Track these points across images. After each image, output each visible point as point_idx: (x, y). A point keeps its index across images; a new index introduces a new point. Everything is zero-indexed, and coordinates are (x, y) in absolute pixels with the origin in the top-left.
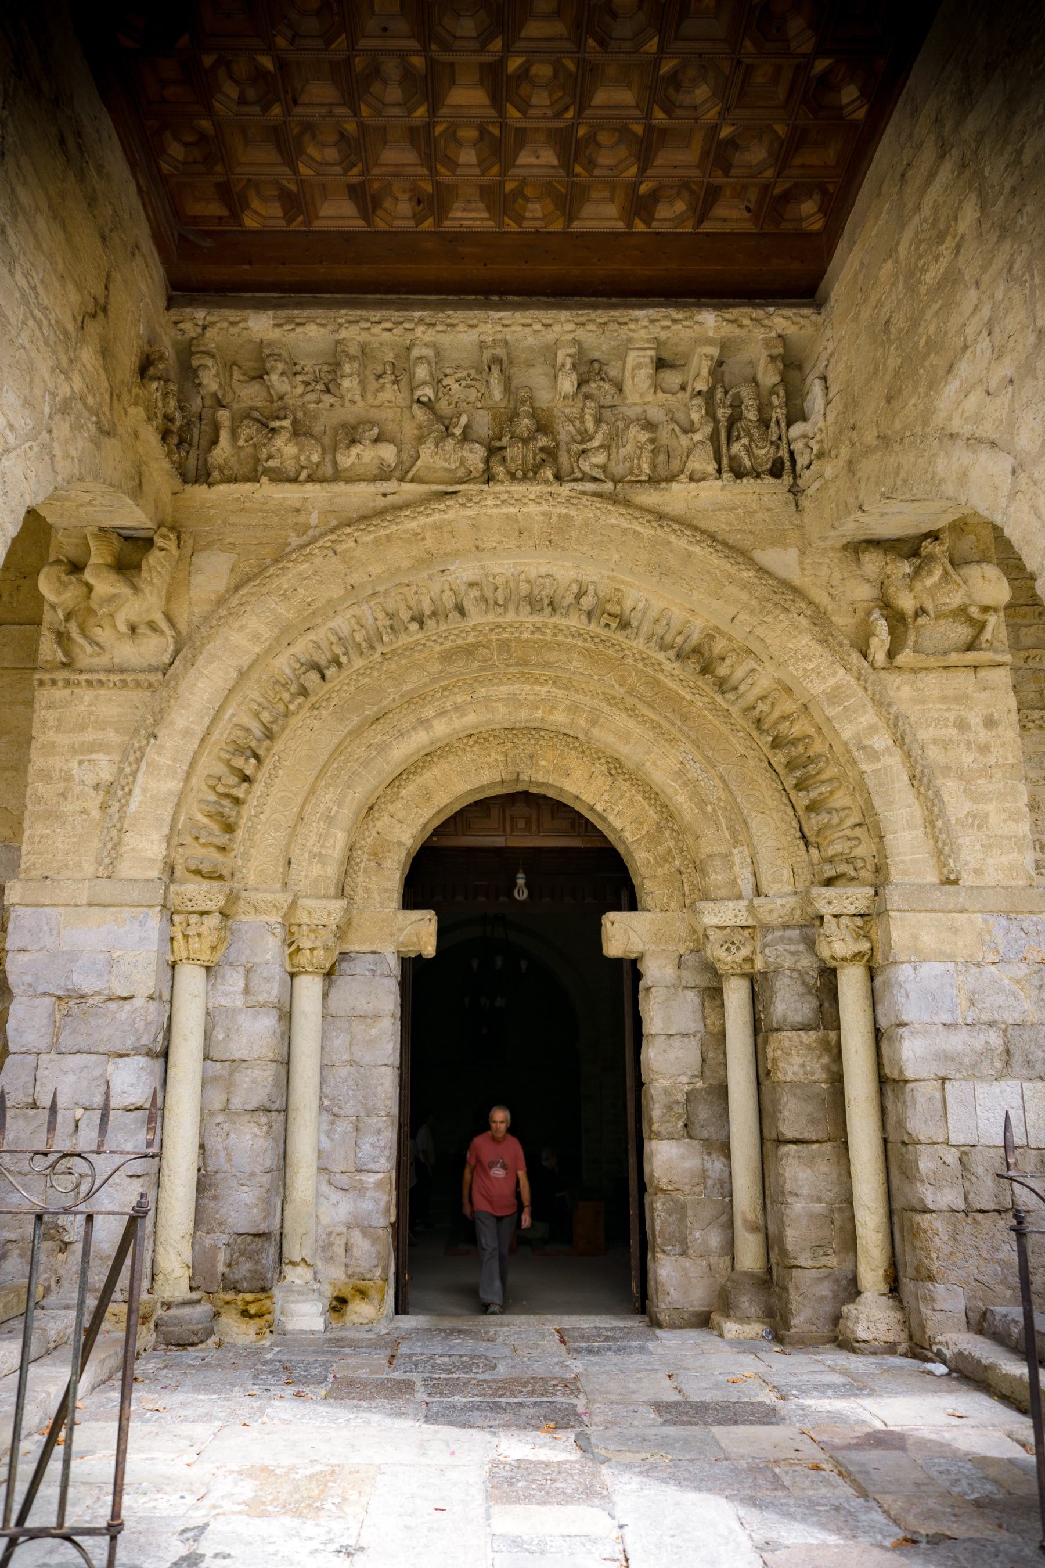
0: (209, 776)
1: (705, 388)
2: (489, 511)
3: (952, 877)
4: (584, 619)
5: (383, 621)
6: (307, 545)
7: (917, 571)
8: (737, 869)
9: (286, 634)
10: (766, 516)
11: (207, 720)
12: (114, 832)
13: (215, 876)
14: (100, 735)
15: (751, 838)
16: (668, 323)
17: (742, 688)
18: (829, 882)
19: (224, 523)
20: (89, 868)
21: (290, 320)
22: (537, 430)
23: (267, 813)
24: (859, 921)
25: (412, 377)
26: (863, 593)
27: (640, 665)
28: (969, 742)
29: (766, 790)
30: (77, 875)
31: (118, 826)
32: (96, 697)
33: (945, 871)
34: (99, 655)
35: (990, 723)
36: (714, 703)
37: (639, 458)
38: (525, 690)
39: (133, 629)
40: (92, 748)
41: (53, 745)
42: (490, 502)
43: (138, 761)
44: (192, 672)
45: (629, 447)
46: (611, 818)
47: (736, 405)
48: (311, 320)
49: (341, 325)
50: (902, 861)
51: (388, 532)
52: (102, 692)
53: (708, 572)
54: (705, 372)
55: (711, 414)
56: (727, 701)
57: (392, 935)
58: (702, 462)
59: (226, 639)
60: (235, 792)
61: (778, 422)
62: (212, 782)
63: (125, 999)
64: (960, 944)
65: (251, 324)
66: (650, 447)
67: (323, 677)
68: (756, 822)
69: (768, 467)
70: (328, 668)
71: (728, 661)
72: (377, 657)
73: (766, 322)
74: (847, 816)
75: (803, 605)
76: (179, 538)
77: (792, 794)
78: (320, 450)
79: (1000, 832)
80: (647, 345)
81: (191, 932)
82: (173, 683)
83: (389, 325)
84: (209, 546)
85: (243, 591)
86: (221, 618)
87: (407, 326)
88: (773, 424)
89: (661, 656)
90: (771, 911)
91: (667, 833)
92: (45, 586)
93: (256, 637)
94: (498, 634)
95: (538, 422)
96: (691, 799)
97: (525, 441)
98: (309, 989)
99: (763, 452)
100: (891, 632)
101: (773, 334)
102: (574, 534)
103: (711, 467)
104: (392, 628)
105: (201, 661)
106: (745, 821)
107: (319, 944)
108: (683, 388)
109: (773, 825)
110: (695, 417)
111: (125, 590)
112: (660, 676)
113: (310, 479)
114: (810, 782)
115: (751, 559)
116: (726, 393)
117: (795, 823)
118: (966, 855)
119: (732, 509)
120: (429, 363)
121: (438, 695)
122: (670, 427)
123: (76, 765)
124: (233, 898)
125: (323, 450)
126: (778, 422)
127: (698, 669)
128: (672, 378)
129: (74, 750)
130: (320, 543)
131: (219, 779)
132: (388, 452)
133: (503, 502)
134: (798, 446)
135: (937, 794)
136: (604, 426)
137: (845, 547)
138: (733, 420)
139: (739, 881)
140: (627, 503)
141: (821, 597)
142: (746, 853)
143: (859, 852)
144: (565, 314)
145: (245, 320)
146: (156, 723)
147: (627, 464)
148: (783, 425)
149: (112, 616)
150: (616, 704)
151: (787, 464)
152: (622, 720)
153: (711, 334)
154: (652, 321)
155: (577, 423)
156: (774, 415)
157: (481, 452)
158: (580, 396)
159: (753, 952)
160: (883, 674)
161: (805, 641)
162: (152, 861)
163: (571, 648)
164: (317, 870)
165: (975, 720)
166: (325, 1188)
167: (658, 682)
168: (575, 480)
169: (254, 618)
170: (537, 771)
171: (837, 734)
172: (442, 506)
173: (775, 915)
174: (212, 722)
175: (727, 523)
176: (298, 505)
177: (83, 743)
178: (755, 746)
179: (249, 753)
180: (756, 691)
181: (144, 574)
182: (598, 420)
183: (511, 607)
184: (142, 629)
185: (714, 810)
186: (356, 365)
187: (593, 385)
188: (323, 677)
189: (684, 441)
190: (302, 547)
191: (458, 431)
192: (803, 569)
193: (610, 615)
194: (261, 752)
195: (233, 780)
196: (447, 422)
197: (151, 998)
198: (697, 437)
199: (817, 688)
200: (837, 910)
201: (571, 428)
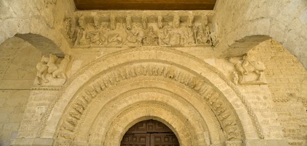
7: (243, 63)
9: (93, 79)
12: (42, 126)
14: (44, 101)
15: (208, 128)
17: (204, 91)
21: (100, 13)
28: (261, 103)
35: (265, 98)
40: (42, 105)
41: (33, 104)
46: (173, 125)
48: (104, 13)
60: (76, 116)
65: (92, 14)
67: (101, 89)
79: (272, 125)
84: (77, 59)
92: (38, 67)
96: (192, 119)
100: (239, 76)
105: (71, 84)
111: (56, 68)
117: (219, 125)
118: (265, 132)
129: (37, 105)
135: (255, 115)
138: (197, 32)
143: (236, 132)
163: (162, 83)
164: (96, 138)
165: (261, 97)
174: (72, 99)
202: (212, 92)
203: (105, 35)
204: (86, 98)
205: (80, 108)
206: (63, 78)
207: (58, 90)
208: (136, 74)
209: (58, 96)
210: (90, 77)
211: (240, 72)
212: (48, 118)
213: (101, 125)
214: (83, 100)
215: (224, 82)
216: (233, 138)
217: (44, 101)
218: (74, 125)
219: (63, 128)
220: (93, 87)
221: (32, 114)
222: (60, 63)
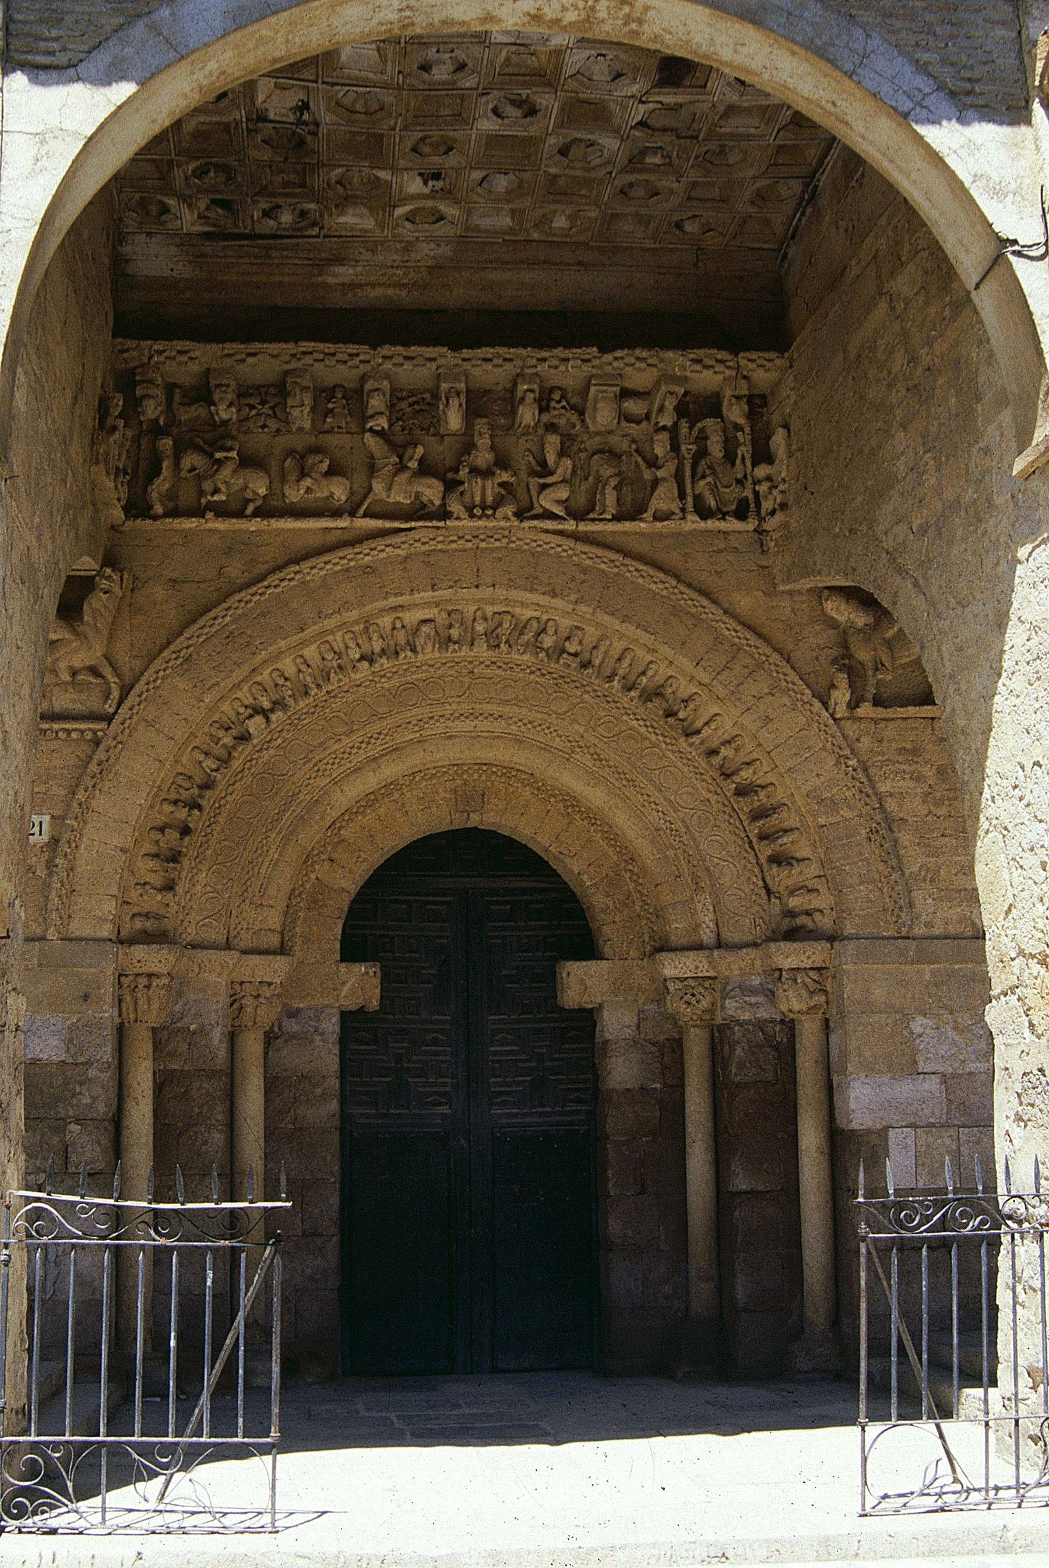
45: (591, 479)
55: (675, 448)
56: (691, 745)
61: (743, 459)
69: (734, 507)
88: (738, 461)
103: (675, 506)
108: (648, 417)
110: (659, 451)
126: (743, 459)
134: (763, 488)
148: (749, 464)
151: (752, 505)
198: (660, 474)
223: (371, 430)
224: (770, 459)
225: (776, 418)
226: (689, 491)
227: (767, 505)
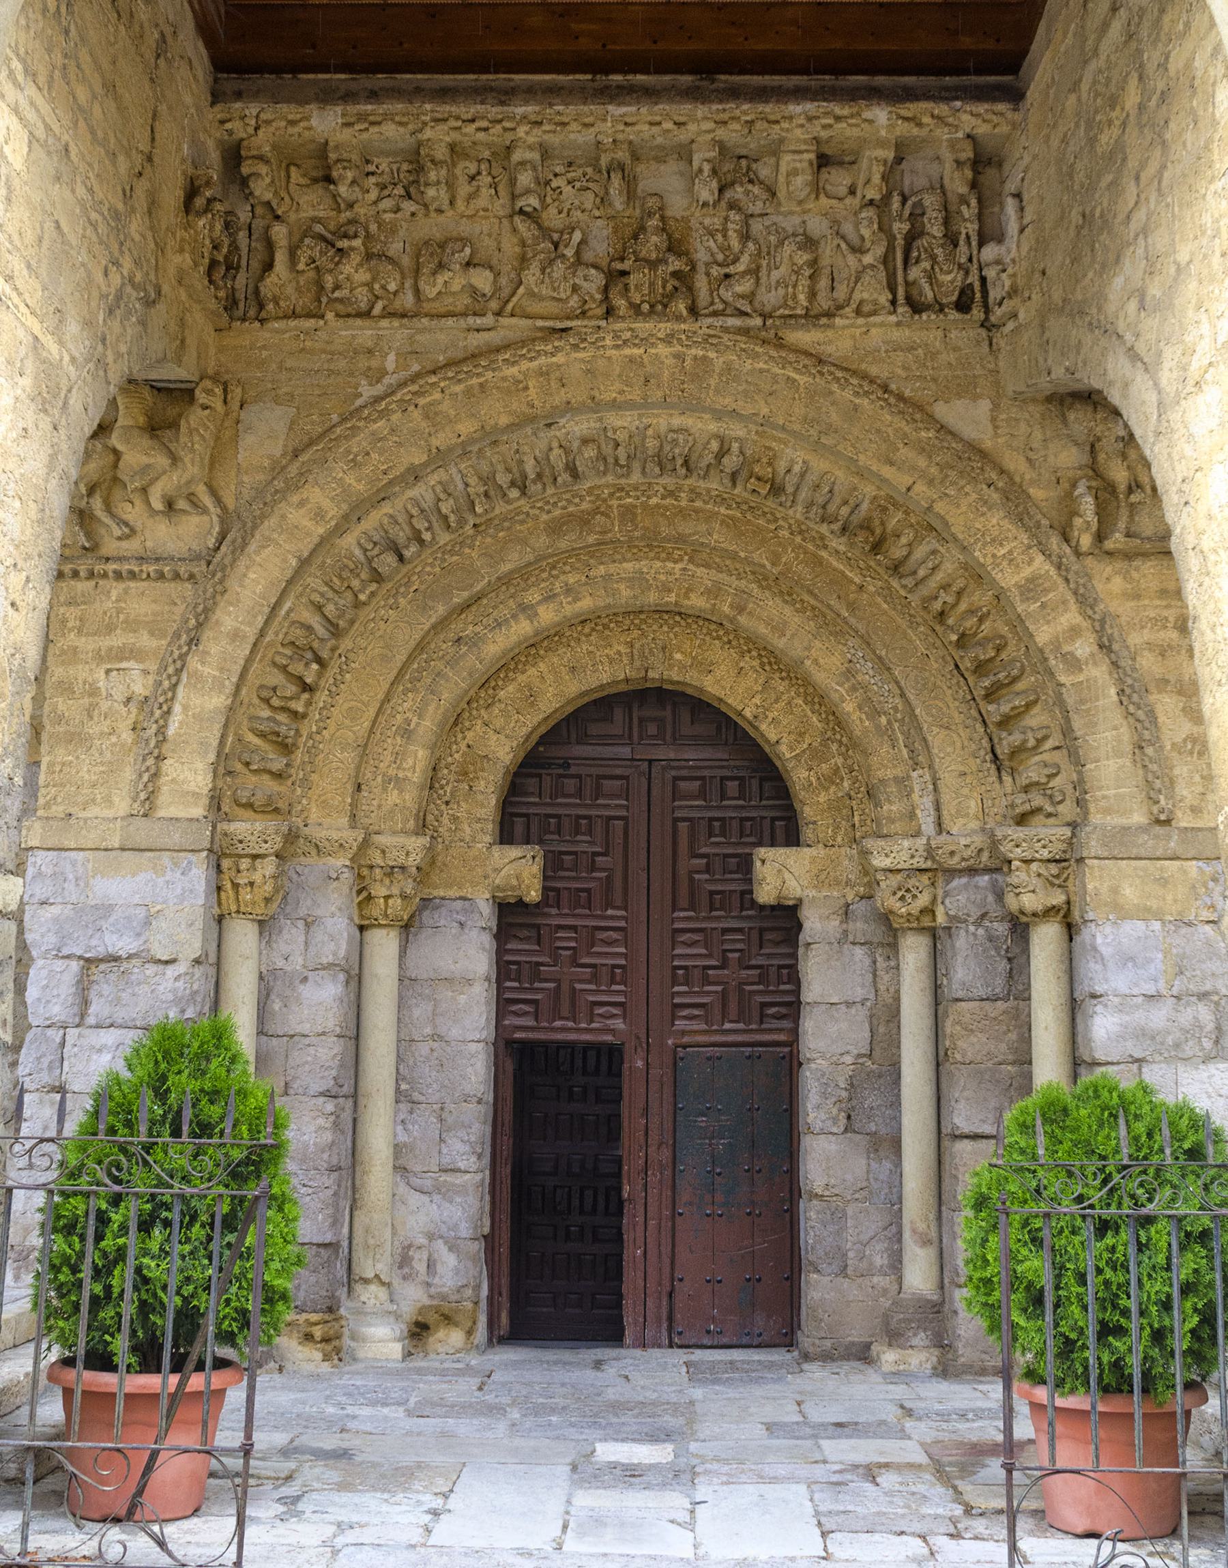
0: (262, 687)
1: (878, 197)
2: (609, 353)
3: (1163, 817)
4: (727, 481)
5: (476, 488)
6: (383, 399)
8: (915, 796)
10: (952, 358)
11: (260, 620)
12: (150, 761)
13: (271, 809)
16: (830, 121)
17: (922, 573)
18: (1022, 820)
19: (280, 368)
20: (122, 805)
21: (362, 117)
22: (669, 249)
23: (332, 729)
24: (1054, 869)
25: (513, 182)
26: (1068, 458)
27: (798, 539)
29: (951, 703)
30: (109, 813)
31: (156, 752)
32: (126, 591)
33: (1155, 809)
34: (127, 537)
36: (889, 588)
37: (795, 286)
38: (652, 568)
39: (170, 505)
40: (124, 653)
42: (608, 342)
43: (178, 672)
44: (242, 563)
45: (783, 269)
47: (916, 216)
49: (425, 124)
50: (1104, 797)
51: (482, 380)
52: (132, 584)
53: (878, 431)
54: (877, 178)
55: (884, 228)
56: (904, 587)
57: (485, 877)
58: (872, 291)
59: (283, 517)
61: (968, 237)
62: (265, 694)
63: (167, 962)
64: (1169, 898)
65: (314, 122)
66: (808, 273)
67: (401, 558)
68: (936, 738)
69: (954, 298)
70: (407, 547)
71: (904, 540)
72: (469, 530)
73: (951, 120)
74: (1046, 738)
75: (994, 476)
76: (225, 391)
77: (982, 704)
78: (398, 277)
80: (804, 147)
81: (242, 881)
82: (219, 575)
83: (484, 124)
85: (304, 458)
86: (277, 491)
87: (507, 124)
88: (962, 243)
89: (824, 529)
90: (952, 853)
91: (834, 747)
93: (319, 515)
94: (620, 498)
95: (670, 237)
97: (653, 265)
98: (384, 945)
99: (949, 278)
101: (960, 135)
102: (713, 382)
103: (884, 298)
104: (486, 495)
105: (252, 547)
106: (925, 740)
107: (396, 891)
109: (959, 744)
110: (866, 233)
111: (162, 461)
112: (824, 554)
113: (388, 314)
114: (1004, 691)
115: (931, 416)
116: (904, 200)
117: (985, 743)
118: (1182, 790)
119: (911, 349)
120: (534, 169)
121: (544, 575)
122: (835, 242)
123: (102, 675)
124: (291, 837)
125: (402, 273)
126: (968, 237)
127: (867, 548)
128: (838, 179)
130: (398, 396)
131: (274, 689)
132: (482, 280)
133: (625, 342)
134: (990, 273)
135: (1152, 715)
136: (750, 244)
137: (1049, 399)
138: (911, 238)
139: (918, 812)
140: (779, 343)
141: (1015, 463)
142: (927, 777)
144: (701, 110)
145: (307, 119)
146: (200, 625)
147: (781, 291)
148: (974, 243)
149: (144, 490)
150: (769, 588)
151: (978, 295)
152: (773, 607)
153: (883, 133)
154: (810, 119)
155: (719, 237)
156: (964, 231)
157: (598, 279)
158: (723, 204)
159: (934, 900)
160: (1089, 561)
161: (996, 520)
162: (195, 795)
163: (712, 516)
166: (402, 1189)
167: (819, 562)
168: (715, 314)
169: (317, 490)
170: (671, 667)
171: (1031, 636)
172: (549, 348)
173: (956, 859)
175: (904, 368)
176: (370, 344)
177: (111, 649)
178: (938, 643)
179: (309, 655)
180: (939, 576)
181: (183, 439)
182: (745, 237)
183: (636, 465)
184: (182, 504)
185: (889, 722)
186: (443, 172)
187: (739, 189)
188: (401, 558)
189: (852, 260)
190: (377, 399)
191: (569, 252)
192: (996, 427)
193: (759, 479)
194: (325, 655)
195: (291, 689)
196: (556, 236)
197: (197, 961)
198: (868, 259)
199: (1008, 579)
200: (1028, 855)
201: (712, 243)
202: (960, 583)
203: (395, 248)
204: (330, 609)
205: (307, 664)
206: (205, 511)
207: (192, 577)
208: (575, 474)
209: (197, 616)
210: (345, 506)
211: (1111, 488)
212: (165, 726)
213: (407, 733)
214: (315, 621)
215: (1024, 537)
216: (1039, 810)
217: (130, 639)
218: (286, 748)
219: (239, 767)
220: (357, 552)
221: (86, 701)
222: (174, 425)
223: (521, 212)
224: (1000, 239)
225: (1011, 186)
226: (900, 279)
227: (994, 294)
